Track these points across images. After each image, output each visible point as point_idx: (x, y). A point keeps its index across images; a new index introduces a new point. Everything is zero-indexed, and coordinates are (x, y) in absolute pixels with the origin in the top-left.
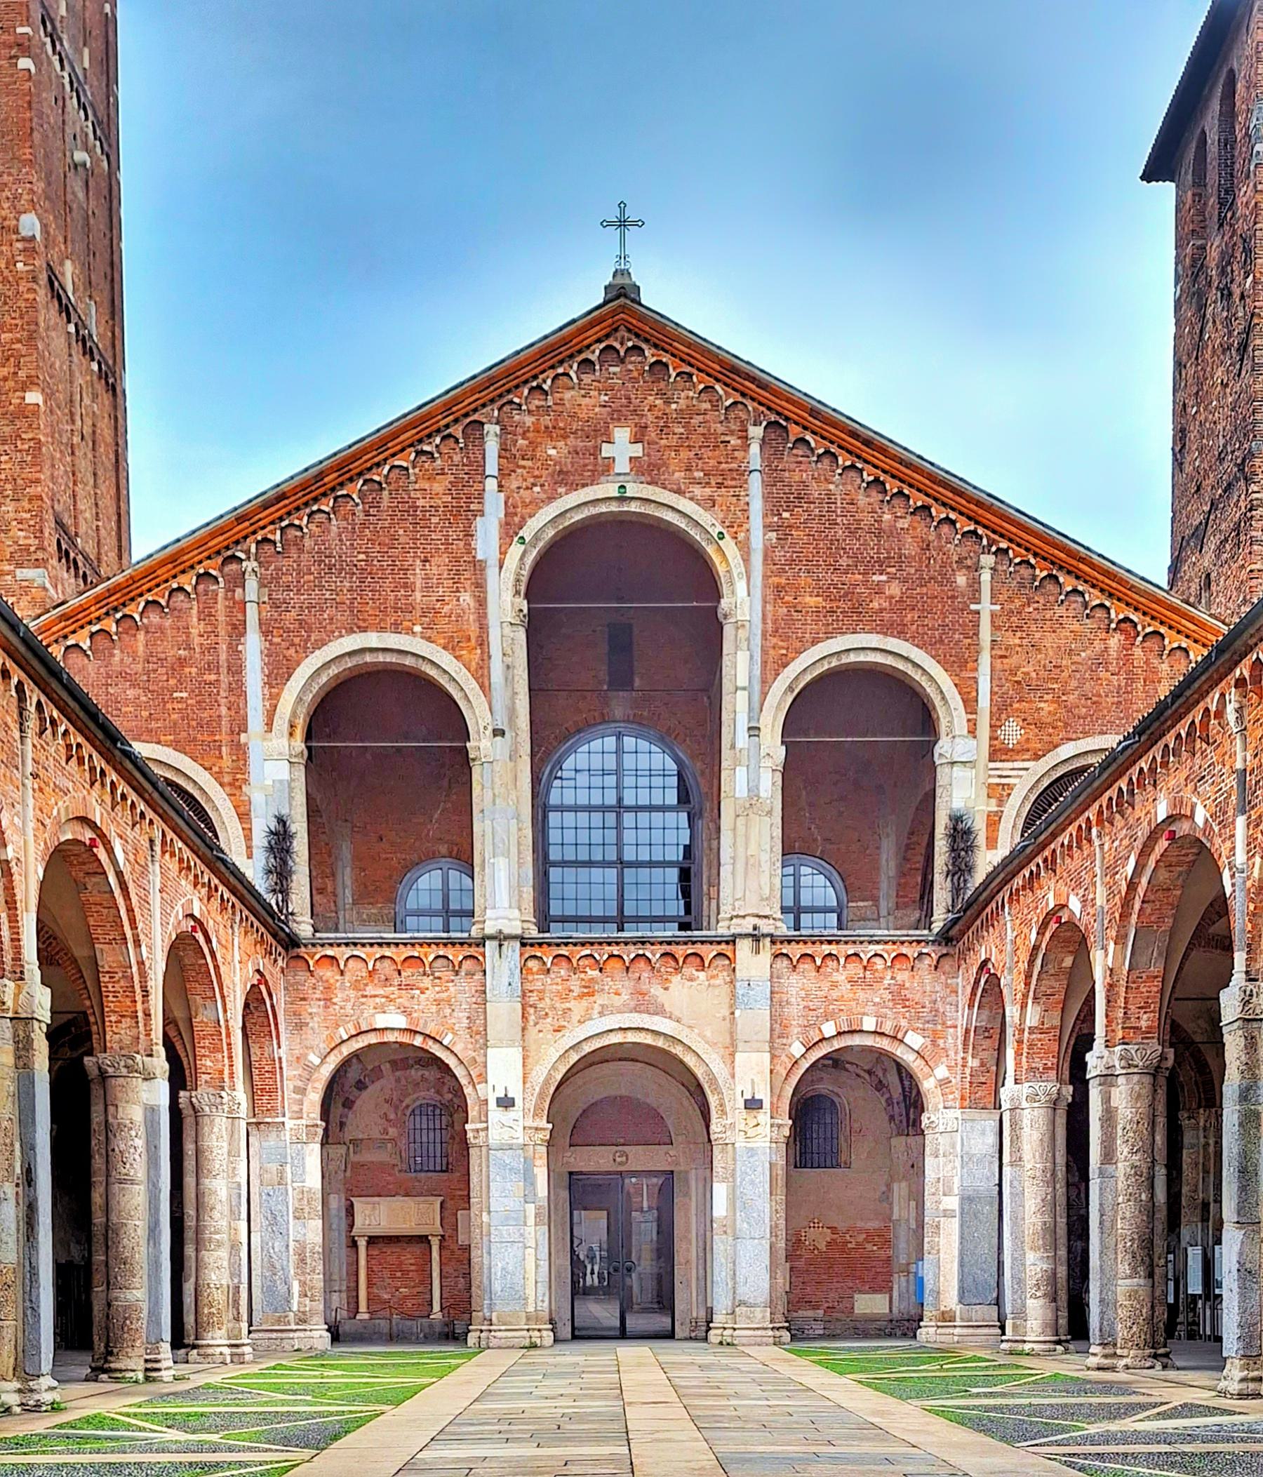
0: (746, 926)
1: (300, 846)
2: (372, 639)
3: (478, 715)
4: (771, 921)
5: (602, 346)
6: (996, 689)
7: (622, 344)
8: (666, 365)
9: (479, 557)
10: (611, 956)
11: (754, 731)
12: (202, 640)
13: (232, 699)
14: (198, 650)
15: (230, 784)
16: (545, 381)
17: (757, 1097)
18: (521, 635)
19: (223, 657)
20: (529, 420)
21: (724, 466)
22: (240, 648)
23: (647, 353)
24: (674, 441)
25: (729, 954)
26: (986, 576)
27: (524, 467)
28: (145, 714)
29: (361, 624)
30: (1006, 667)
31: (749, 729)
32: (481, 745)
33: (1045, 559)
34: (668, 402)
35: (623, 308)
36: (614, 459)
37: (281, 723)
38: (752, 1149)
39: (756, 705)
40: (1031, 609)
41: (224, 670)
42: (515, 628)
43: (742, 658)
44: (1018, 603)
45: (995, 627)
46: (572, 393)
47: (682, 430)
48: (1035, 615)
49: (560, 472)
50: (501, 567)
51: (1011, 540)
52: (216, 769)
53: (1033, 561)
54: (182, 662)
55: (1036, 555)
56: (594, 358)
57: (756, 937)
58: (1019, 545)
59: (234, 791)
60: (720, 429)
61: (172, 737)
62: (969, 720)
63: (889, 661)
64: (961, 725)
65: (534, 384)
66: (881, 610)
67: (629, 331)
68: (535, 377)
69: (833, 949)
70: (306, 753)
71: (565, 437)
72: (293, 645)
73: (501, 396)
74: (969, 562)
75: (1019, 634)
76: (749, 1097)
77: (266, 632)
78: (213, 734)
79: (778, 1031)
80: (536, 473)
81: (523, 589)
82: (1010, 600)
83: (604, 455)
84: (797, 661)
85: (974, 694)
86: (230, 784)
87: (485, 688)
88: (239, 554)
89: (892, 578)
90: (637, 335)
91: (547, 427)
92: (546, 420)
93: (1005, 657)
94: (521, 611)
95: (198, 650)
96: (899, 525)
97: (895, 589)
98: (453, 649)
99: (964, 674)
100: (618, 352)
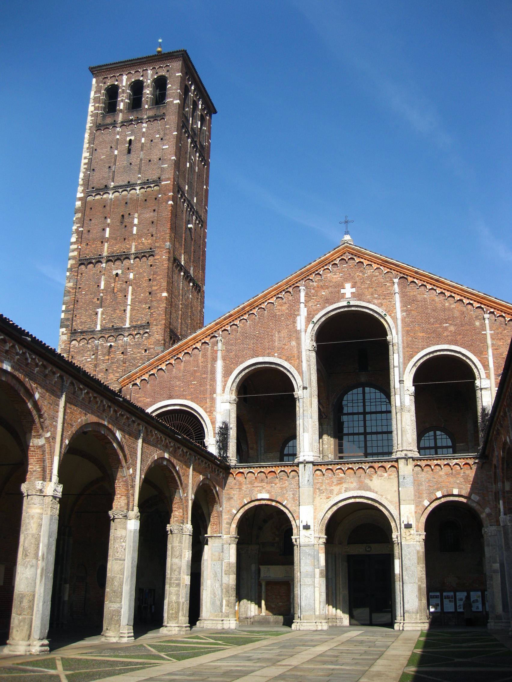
0: (403, 454)
1: (233, 433)
2: (260, 359)
3: (298, 382)
4: (413, 452)
5: (340, 259)
6: (495, 361)
7: (347, 257)
8: (362, 263)
9: (298, 328)
10: (349, 468)
11: (401, 382)
12: (202, 364)
13: (212, 383)
14: (201, 367)
15: (210, 412)
16: (320, 272)
17: (409, 523)
18: (314, 354)
19: (209, 369)
20: (315, 284)
21: (384, 293)
22: (215, 365)
23: (355, 259)
24: (367, 286)
25: (396, 466)
26: (487, 321)
27: (314, 299)
28: (182, 389)
29: (256, 354)
30: (498, 353)
31: (400, 381)
32: (298, 393)
33: (508, 314)
34: (364, 274)
35: (347, 247)
36: (345, 293)
37: (227, 389)
38: (408, 545)
39: (402, 372)
40: (506, 332)
41: (209, 373)
42: (311, 352)
43: (396, 356)
44: (500, 330)
45: (493, 339)
46: (331, 274)
47: (369, 282)
48: (507, 334)
49: (327, 299)
50: (306, 332)
51: (495, 309)
52: (204, 407)
53: (504, 315)
54: (195, 371)
55: (505, 313)
56: (337, 263)
57: (406, 458)
58: (498, 310)
59: (210, 414)
60: (382, 280)
61: (190, 397)
62: (486, 373)
63: (453, 354)
64: (483, 375)
65: (317, 273)
66: (448, 336)
67: (349, 253)
68: (317, 271)
69: (439, 462)
70: (237, 400)
71: (328, 288)
72: (233, 363)
73: (305, 277)
74: (480, 317)
75: (502, 341)
76: (406, 523)
77: (224, 359)
78: (204, 395)
79: (418, 496)
80: (318, 300)
81: (314, 338)
82: (497, 329)
83: (342, 292)
84: (417, 356)
85: (487, 363)
86: (210, 412)
87: (301, 373)
88: (216, 335)
89: (451, 324)
90: (352, 254)
91: (321, 286)
92: (321, 283)
93: (497, 349)
94: (313, 346)
95: (201, 367)
96: (452, 307)
97: (452, 328)
98: (289, 360)
99: (482, 356)
100: (345, 260)
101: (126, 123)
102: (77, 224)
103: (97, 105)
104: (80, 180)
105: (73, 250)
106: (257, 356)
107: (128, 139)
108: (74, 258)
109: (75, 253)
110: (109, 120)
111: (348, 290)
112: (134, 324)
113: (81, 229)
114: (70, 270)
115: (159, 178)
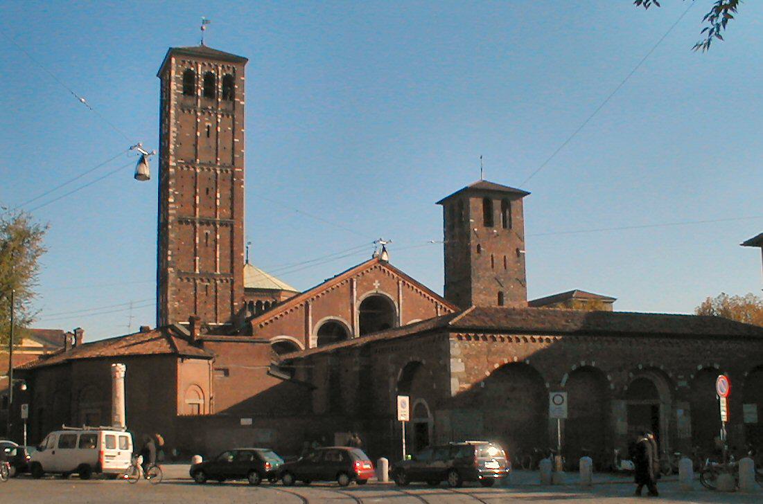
2: (332, 318)
97: (423, 311)
101: (204, 110)
102: (174, 187)
103: (178, 85)
104: (171, 151)
105: (172, 209)
106: (330, 315)
107: (207, 124)
108: (173, 215)
109: (174, 212)
110: (189, 102)
111: (376, 284)
112: (223, 272)
113: (176, 193)
114: (172, 224)
115: (233, 164)
